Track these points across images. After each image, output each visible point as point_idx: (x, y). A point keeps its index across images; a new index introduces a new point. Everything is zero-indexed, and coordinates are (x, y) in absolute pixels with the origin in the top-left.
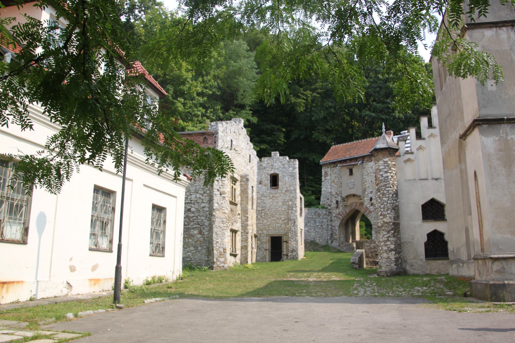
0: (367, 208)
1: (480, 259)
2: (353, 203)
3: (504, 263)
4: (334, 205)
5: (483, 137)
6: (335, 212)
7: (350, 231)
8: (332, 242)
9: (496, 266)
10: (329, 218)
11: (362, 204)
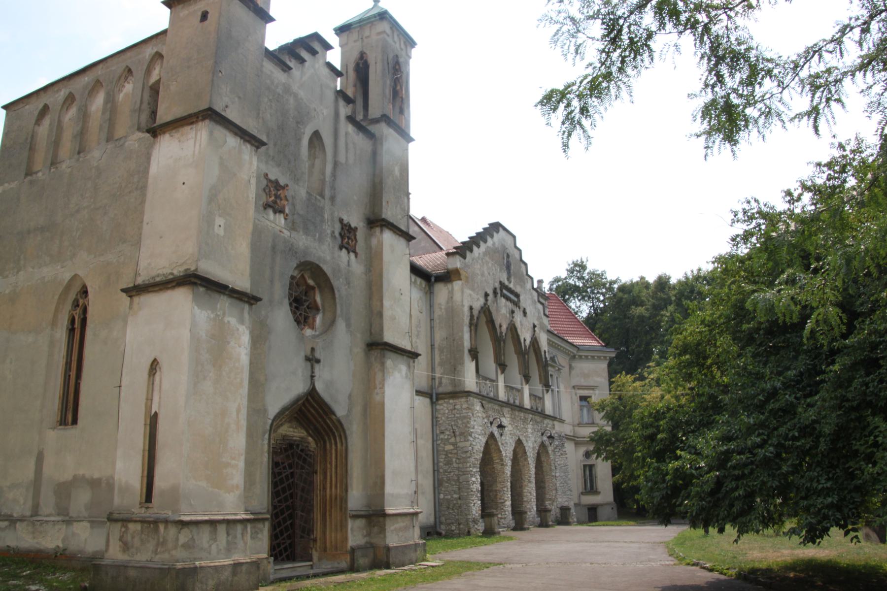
1: (136, 521)
3: (194, 529)
5: (196, 307)
9: (184, 536)
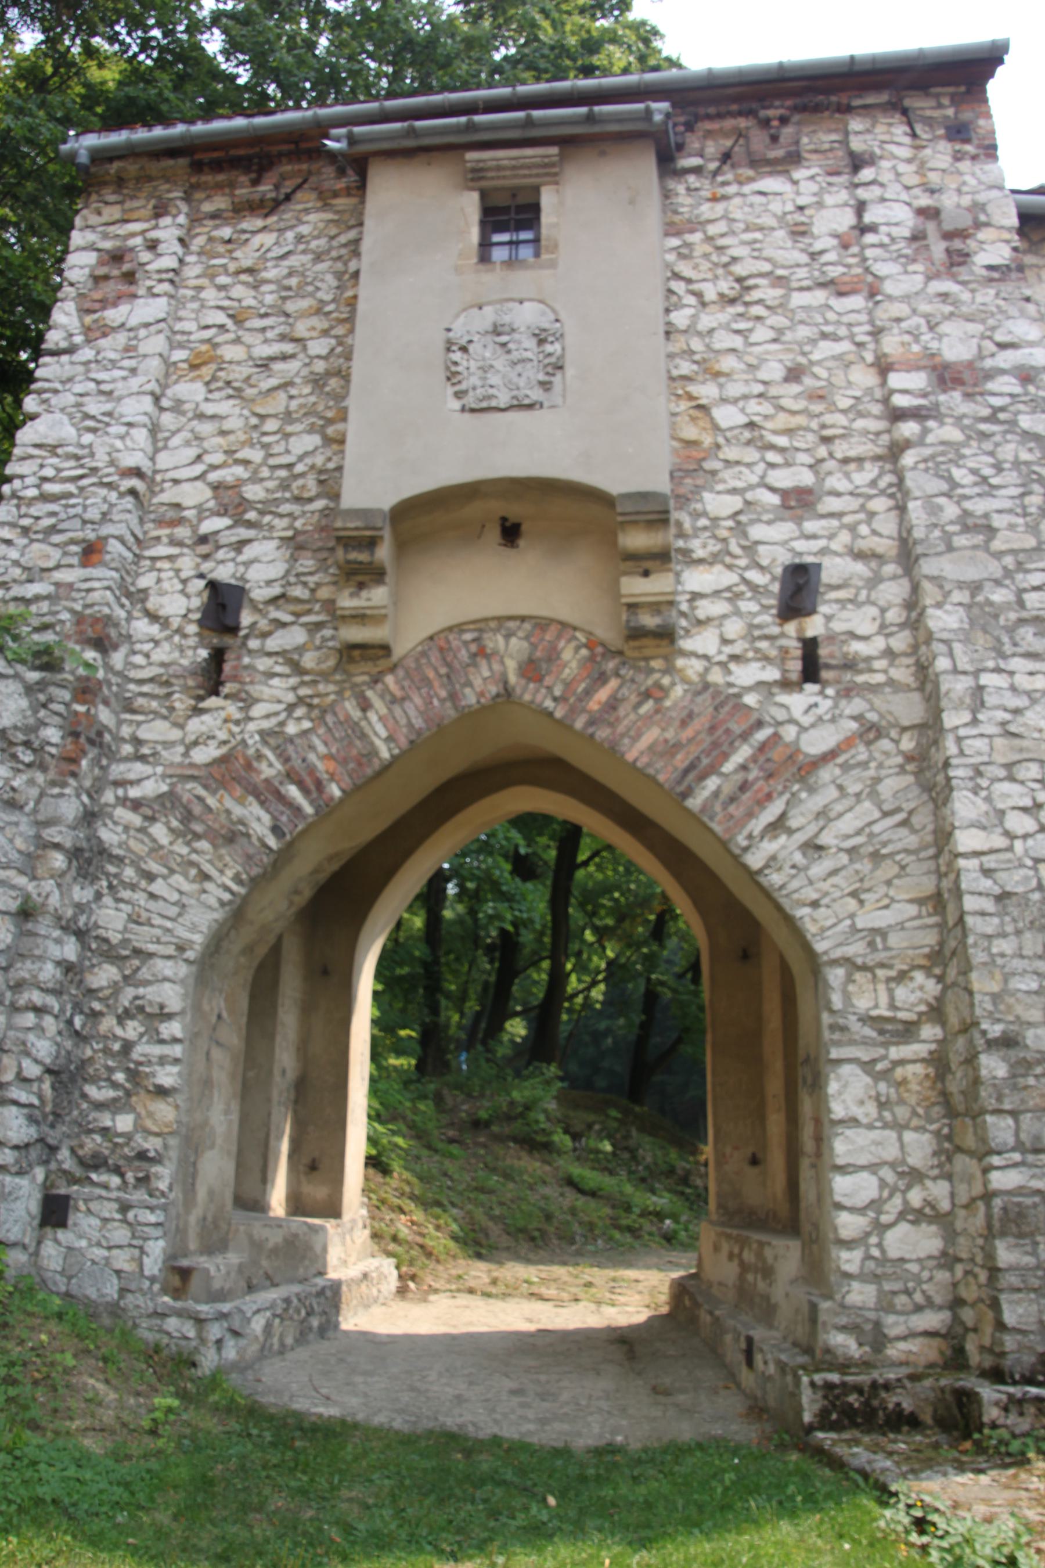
0: (726, 716)
2: (481, 625)
4: (162, 640)
6: (172, 740)
7: (286, 1059)
8: (55, 1212)
10: (70, 808)
11: (652, 636)
